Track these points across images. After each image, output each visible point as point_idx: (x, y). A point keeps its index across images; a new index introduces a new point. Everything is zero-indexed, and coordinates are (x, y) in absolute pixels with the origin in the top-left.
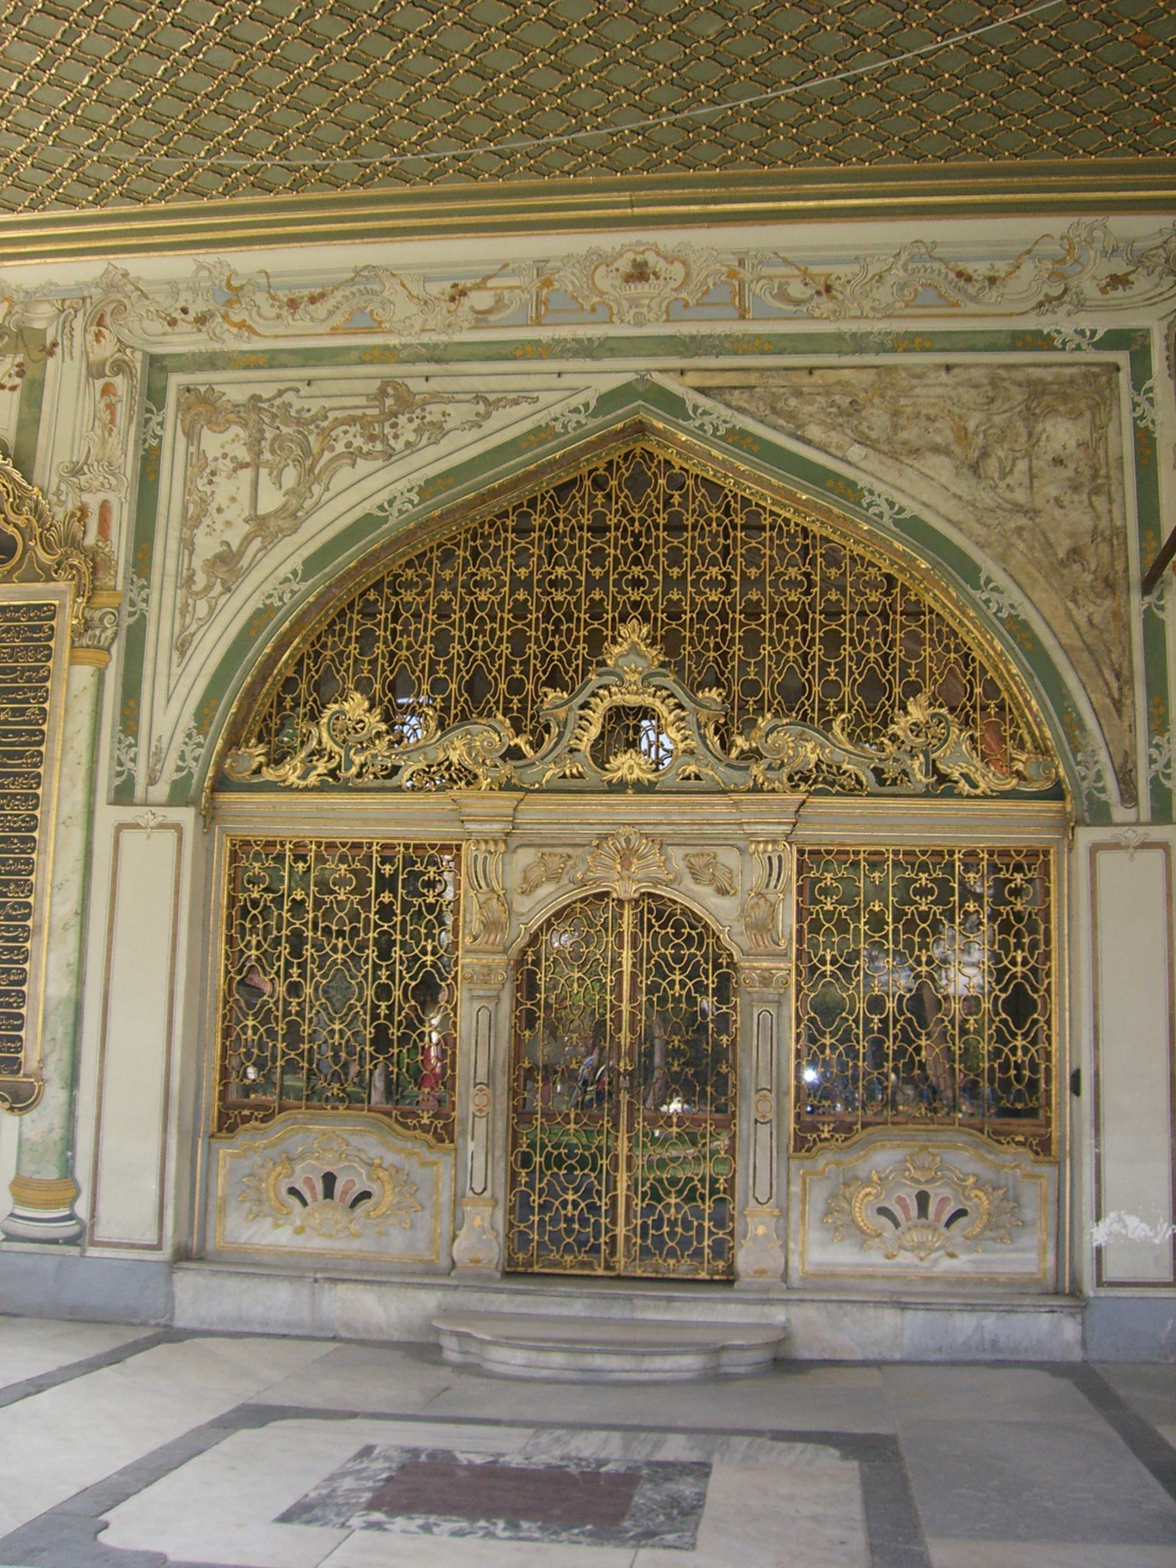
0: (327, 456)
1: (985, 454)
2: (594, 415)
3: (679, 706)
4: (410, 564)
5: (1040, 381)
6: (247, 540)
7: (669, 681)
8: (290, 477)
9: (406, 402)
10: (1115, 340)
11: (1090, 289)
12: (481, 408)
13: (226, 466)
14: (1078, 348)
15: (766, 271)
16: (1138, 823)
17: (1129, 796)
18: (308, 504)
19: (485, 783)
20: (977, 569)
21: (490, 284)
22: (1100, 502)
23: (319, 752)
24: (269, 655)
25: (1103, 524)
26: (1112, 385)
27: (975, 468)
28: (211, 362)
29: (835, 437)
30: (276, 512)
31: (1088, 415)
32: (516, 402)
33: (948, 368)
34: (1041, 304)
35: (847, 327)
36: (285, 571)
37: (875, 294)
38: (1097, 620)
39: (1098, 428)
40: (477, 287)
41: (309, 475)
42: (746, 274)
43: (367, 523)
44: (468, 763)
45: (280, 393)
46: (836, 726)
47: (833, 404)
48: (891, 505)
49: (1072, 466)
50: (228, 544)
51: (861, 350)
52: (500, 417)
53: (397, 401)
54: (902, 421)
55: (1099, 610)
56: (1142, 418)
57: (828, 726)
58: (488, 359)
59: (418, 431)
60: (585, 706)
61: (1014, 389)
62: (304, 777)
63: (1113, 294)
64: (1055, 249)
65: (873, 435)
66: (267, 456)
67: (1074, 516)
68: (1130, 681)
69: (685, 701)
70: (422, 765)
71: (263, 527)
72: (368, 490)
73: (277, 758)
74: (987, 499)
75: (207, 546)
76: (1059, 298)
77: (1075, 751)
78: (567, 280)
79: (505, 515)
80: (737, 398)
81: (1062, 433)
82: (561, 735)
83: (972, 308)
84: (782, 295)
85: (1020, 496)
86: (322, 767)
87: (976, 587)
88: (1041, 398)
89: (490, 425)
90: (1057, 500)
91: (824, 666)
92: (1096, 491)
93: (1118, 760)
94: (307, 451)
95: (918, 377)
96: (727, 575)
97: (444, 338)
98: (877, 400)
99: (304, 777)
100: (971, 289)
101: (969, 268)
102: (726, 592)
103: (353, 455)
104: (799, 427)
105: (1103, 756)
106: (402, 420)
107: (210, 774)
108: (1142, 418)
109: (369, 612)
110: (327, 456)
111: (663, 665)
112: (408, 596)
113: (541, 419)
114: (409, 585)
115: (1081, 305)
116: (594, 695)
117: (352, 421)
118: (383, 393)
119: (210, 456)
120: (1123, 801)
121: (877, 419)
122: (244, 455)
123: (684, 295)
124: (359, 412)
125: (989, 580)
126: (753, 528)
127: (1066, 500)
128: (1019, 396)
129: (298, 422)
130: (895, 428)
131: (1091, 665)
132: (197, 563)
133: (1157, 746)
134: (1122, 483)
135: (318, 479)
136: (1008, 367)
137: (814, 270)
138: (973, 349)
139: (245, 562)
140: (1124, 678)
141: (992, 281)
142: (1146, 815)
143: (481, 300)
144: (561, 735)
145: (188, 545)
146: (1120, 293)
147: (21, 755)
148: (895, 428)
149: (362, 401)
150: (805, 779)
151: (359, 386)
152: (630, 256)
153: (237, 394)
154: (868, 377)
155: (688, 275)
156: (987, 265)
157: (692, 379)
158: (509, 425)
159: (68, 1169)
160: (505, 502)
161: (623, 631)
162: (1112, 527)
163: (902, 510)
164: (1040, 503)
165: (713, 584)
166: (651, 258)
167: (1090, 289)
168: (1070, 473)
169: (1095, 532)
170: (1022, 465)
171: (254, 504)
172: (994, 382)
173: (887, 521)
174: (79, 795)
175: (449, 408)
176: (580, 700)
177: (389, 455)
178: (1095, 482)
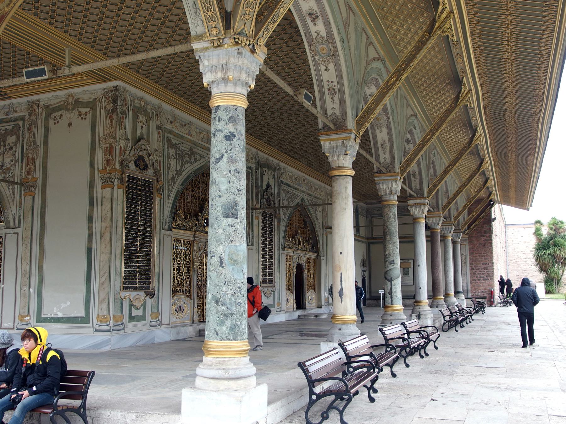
8: (180, 162)
9: (193, 153)
13: (173, 158)
23: (176, 221)
28: (170, 132)
43: (188, 177)
52: (203, 160)
75: (171, 176)
89: (201, 161)
103: (187, 161)
117: (187, 154)
119: (171, 154)
129: (181, 151)
145: (168, 173)
147: (149, 216)
159: (158, 310)
174: (159, 227)
177: (191, 163)
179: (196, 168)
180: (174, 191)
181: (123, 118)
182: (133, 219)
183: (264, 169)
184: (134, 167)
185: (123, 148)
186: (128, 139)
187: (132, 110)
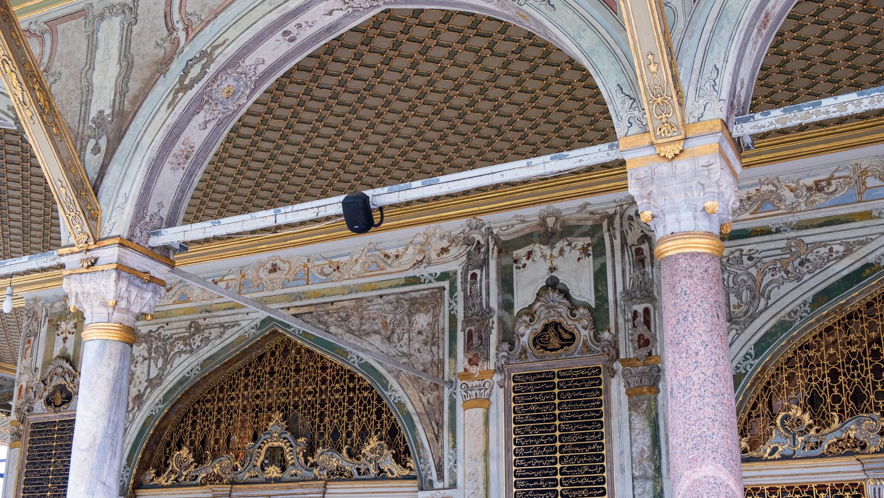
0: (172, 353)
1: (393, 332)
2: (258, 329)
3: (291, 446)
4: (209, 392)
5: (415, 298)
6: (146, 388)
7: (288, 435)
8: (160, 363)
10: (444, 276)
11: (434, 256)
12: (222, 330)
13: (140, 359)
14: (430, 281)
15: (317, 263)
16: (444, 489)
17: (441, 477)
18: (166, 372)
19: (225, 481)
20: (388, 382)
21: (226, 278)
22: (435, 349)
24: (153, 434)
25: (436, 358)
26: (442, 297)
27: (389, 339)
29: (340, 331)
30: (155, 378)
31: (432, 311)
32: (233, 326)
33: (381, 296)
34: (414, 265)
35: (345, 283)
36: (157, 401)
37: (355, 268)
38: (431, 400)
39: (435, 316)
40: (221, 280)
41: (166, 362)
42: (310, 265)
44: (220, 473)
45: (158, 329)
46: (344, 451)
47: (340, 316)
48: (358, 357)
49: (425, 334)
50: (139, 391)
51: (351, 292)
52: (229, 332)
53: (195, 328)
54: (364, 321)
55: (432, 396)
56: (452, 310)
57: (339, 450)
58: (225, 309)
59: (201, 341)
60: (260, 447)
61: (405, 303)
62: (167, 481)
63: (442, 256)
64: (421, 239)
65: (353, 328)
66: (153, 355)
67: (425, 356)
68: (442, 427)
69: (294, 445)
70: (205, 475)
71: (152, 383)
72: (184, 366)
73: (158, 474)
74: (393, 352)
76: (421, 261)
77: (420, 458)
78: (250, 274)
79: (240, 370)
80: (307, 317)
81: (422, 320)
82: (251, 460)
83: (389, 270)
84: (322, 273)
85: (405, 349)
86: (173, 477)
87: (387, 390)
88: (415, 305)
89: (225, 336)
90: (419, 349)
91: (347, 425)
92: (433, 344)
93: (437, 461)
94: (166, 352)
95: (370, 301)
96: (314, 389)
97: (210, 302)
98: (355, 313)
99: (167, 481)
100: (389, 262)
101: (389, 252)
102: (314, 396)
104: (327, 327)
105: (431, 460)
106: (196, 336)
107: (132, 482)
108: (452, 310)
109: (195, 414)
110: (172, 353)
111: (287, 429)
112: (208, 405)
113: (241, 332)
114: (208, 401)
115: (429, 264)
116: (263, 443)
118: (190, 325)
119: (136, 355)
120: (438, 479)
121: (355, 320)
122: (147, 355)
123: (288, 277)
124: (182, 335)
125: (391, 386)
126: (324, 368)
127: (422, 349)
128: (406, 305)
130: (361, 324)
131: (427, 421)
132: (130, 399)
133: (452, 454)
134: (443, 340)
135: (169, 363)
136: (403, 293)
137: (334, 260)
138: (390, 287)
139: (145, 398)
140: (440, 425)
141: (397, 256)
142: (447, 485)
143: (222, 285)
144: (251, 460)
146: (445, 255)
148: (361, 324)
149: (183, 330)
150: (333, 474)
151: (183, 324)
152: (271, 262)
153: (144, 330)
154: (353, 303)
155: (290, 268)
156: (395, 250)
157: (292, 311)
158: (231, 336)
160: (239, 364)
161: (273, 416)
162: (439, 359)
163: (362, 359)
164: (412, 351)
165: (310, 393)
166: (278, 262)
167: (434, 256)
168: (424, 337)
169: (432, 362)
170: (406, 336)
171: (149, 375)
172: (398, 301)
173: (356, 365)
175: (212, 331)
176: (258, 445)
177: (191, 351)
178: (433, 341)
179: (205, 357)
180: (138, 420)
181: (29, 342)
182: (37, 488)
183: (521, 252)
184: (44, 407)
185: (24, 387)
186: (36, 369)
187: (47, 323)
